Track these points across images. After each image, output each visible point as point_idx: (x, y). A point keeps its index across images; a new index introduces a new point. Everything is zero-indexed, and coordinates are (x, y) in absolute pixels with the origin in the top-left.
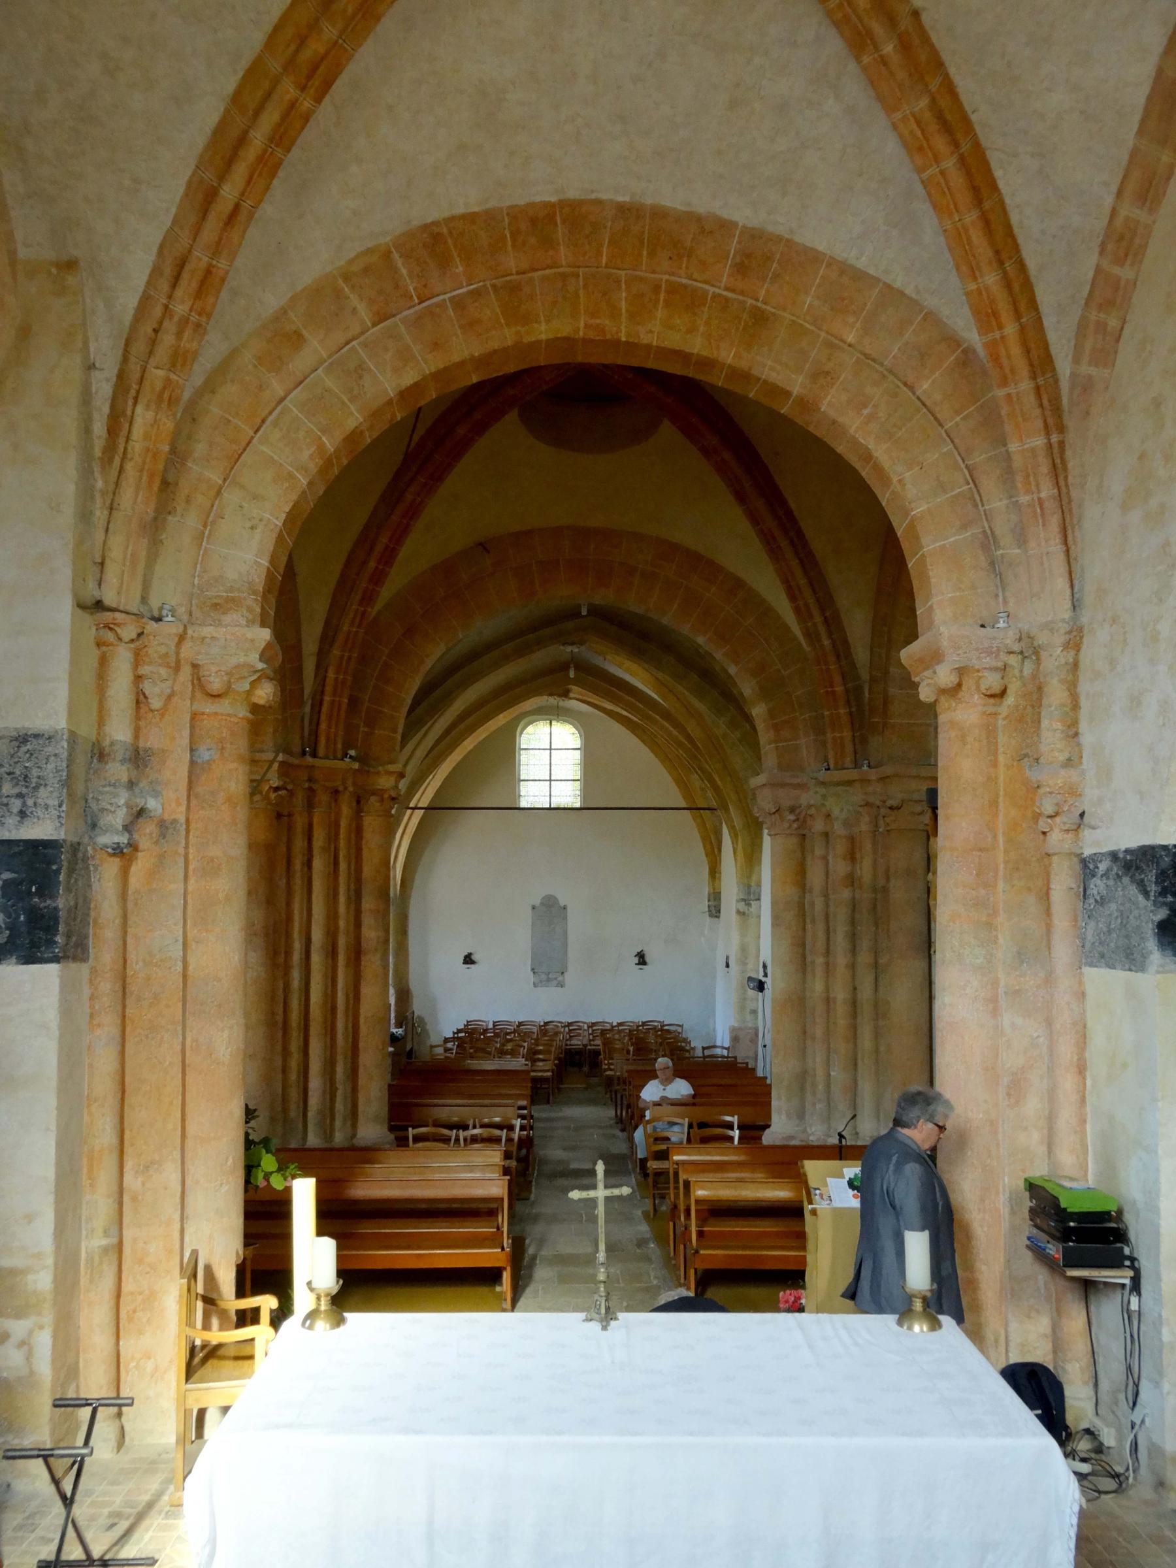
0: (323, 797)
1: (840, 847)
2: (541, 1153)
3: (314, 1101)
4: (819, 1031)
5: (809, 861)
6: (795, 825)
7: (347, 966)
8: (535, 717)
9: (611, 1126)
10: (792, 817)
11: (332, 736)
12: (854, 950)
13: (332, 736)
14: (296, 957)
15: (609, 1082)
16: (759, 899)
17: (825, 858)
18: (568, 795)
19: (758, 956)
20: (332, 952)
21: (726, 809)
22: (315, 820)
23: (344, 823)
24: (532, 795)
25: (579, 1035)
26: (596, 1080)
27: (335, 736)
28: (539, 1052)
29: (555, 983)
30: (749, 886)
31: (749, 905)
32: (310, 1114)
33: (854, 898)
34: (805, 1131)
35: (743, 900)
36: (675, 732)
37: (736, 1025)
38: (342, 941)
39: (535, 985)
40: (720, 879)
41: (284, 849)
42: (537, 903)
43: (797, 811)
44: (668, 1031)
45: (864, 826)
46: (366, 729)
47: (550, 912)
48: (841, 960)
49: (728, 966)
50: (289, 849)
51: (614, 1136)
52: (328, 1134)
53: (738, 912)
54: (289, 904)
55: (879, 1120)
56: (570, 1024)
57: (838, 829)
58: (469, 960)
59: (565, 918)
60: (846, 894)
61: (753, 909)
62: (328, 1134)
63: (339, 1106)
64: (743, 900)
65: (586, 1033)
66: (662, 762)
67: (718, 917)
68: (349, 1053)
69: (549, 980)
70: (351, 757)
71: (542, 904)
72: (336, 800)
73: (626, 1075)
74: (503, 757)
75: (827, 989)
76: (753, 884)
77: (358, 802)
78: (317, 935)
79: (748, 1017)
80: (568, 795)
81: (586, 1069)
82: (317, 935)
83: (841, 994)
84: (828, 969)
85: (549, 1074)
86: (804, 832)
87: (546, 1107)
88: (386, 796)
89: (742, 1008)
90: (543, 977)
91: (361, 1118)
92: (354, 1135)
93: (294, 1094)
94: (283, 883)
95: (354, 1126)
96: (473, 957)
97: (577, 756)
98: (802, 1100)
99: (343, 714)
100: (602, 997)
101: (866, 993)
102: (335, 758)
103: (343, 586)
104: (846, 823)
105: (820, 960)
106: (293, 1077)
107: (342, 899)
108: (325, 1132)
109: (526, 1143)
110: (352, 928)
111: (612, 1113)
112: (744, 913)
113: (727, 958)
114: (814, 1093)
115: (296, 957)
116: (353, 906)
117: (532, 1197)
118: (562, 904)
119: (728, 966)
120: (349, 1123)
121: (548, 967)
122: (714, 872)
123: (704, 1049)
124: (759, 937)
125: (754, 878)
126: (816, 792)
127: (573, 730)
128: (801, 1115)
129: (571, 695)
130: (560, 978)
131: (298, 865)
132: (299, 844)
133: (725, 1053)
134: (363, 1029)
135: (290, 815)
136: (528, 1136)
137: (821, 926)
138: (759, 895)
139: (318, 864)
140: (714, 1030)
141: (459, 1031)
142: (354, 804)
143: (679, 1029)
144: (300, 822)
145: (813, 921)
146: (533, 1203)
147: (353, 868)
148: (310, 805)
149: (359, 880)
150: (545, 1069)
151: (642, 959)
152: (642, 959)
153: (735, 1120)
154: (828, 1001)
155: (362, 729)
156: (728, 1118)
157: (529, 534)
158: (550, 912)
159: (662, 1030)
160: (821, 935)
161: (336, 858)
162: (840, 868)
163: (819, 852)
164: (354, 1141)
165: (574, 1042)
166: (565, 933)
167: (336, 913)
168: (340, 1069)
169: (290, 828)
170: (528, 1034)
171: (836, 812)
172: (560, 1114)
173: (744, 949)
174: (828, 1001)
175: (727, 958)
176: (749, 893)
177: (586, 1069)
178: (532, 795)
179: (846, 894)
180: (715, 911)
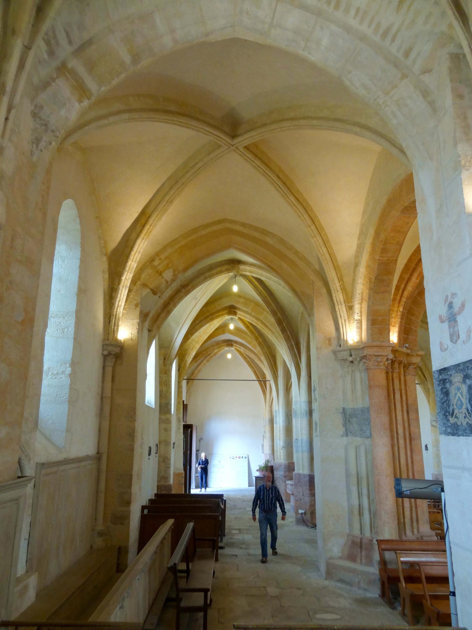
35: (435, 421)
46: (405, 336)
53: (432, 426)
64: (435, 421)
70: (406, 347)
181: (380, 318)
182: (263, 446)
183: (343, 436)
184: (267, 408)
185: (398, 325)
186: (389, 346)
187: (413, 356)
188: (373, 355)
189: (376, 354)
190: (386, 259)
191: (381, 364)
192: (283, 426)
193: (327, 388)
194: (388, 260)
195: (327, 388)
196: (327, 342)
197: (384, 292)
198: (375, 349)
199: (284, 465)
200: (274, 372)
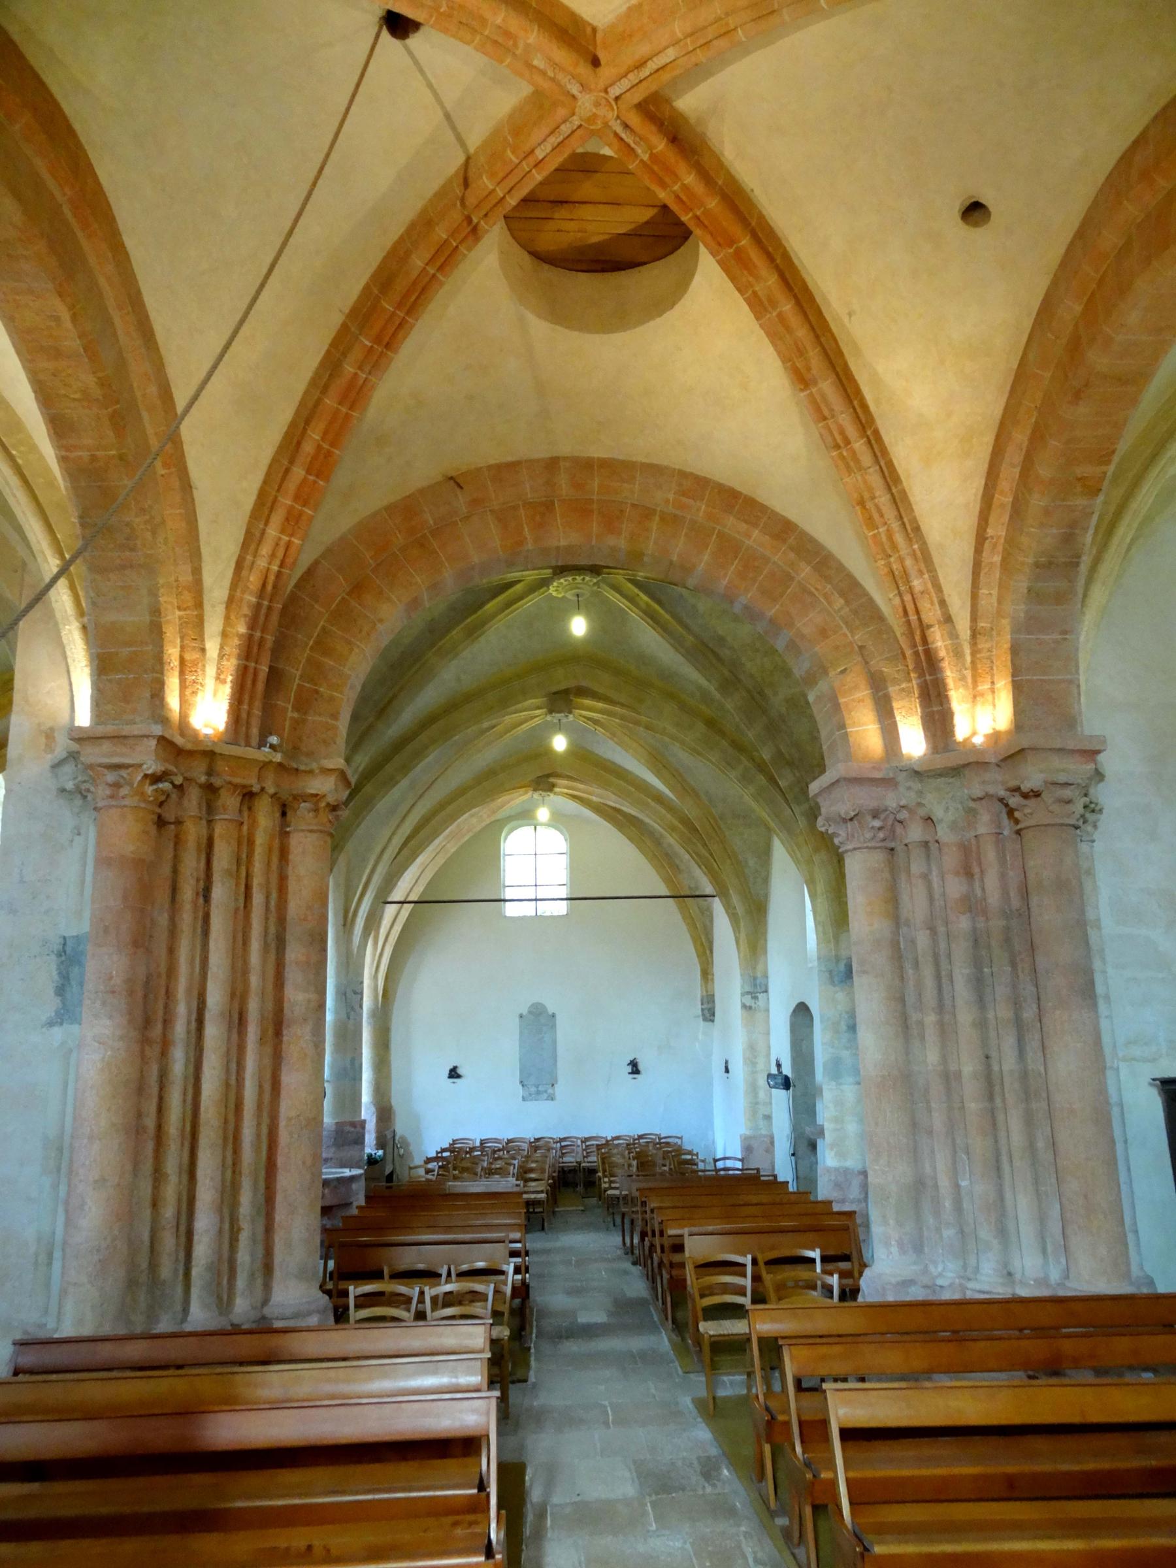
0: (229, 802)
1: (951, 859)
2: (539, 1299)
3: (202, 1250)
4: (938, 1121)
5: (903, 884)
6: (881, 835)
7: (262, 1040)
8: (520, 822)
9: (619, 1258)
10: (877, 823)
11: (244, 715)
12: (981, 1002)
13: (244, 715)
14: (180, 1028)
15: (612, 1204)
16: (766, 991)
17: (926, 877)
19: (768, 1055)
20: (238, 1021)
22: (219, 830)
23: (260, 839)
25: (572, 1151)
26: (594, 1201)
27: (249, 714)
28: (532, 1170)
29: (545, 1096)
30: (755, 979)
31: (755, 998)
32: (195, 1272)
33: (974, 930)
34: (925, 1271)
35: (748, 993)
36: (669, 816)
37: (748, 1133)
38: (253, 1007)
39: (524, 1099)
40: (713, 980)
41: (166, 870)
42: (525, 1012)
43: (882, 816)
44: (668, 1144)
45: (984, 825)
46: (296, 715)
47: (538, 1022)
48: (965, 1016)
49: (727, 1071)
50: (175, 871)
51: (626, 1272)
52: (223, 1303)
53: (744, 1006)
54: (171, 951)
55: (1044, 1251)
56: (564, 1139)
57: (944, 833)
58: (454, 1074)
59: (554, 1026)
60: (964, 923)
61: (761, 1002)
62: (223, 1303)
63: (244, 1257)
64: (748, 993)
65: (580, 1149)
66: (651, 861)
67: (713, 1021)
68: (262, 1174)
69: (538, 1093)
70: (272, 747)
71: (530, 1012)
72: (250, 809)
73: (637, 1194)
74: (484, 854)
75: (944, 1059)
76: (759, 975)
77: (284, 814)
78: (215, 998)
79: (762, 1123)
81: (580, 1189)
82: (215, 998)
83: (968, 1067)
84: (946, 1031)
85: (543, 1195)
86: (892, 845)
87: (543, 1234)
88: (323, 804)
89: (754, 1112)
90: (533, 1089)
91: (277, 1273)
92: (266, 1302)
93: (168, 1241)
94: (163, 920)
95: (267, 1287)
96: (459, 1071)
97: (564, 861)
98: (918, 1219)
99: (260, 686)
100: (598, 1110)
101: (1008, 1063)
102: (248, 745)
103: (264, 505)
104: (954, 826)
105: (931, 1019)
106: (169, 1212)
107: (255, 945)
108: (219, 1298)
109: (522, 1291)
110: (270, 987)
111: (618, 1239)
112: (750, 1008)
113: (726, 1062)
114: (937, 1213)
115: (180, 1028)
116: (272, 957)
117: (532, 1378)
119: (727, 1071)
120: (259, 1281)
121: (538, 1079)
124: (768, 1034)
125: (760, 967)
126: (909, 788)
128: (918, 1246)
129: (557, 790)
130: (550, 1091)
131: (188, 892)
132: (191, 864)
133: (739, 1165)
134: (284, 1137)
135: (179, 822)
136: (523, 1281)
137: (928, 972)
139: (220, 892)
140: (713, 1142)
141: (443, 1150)
142: (278, 815)
143: (679, 1141)
144: (193, 832)
145: (916, 965)
146: (534, 1385)
147: (273, 903)
148: (210, 808)
149: (282, 921)
150: (538, 1190)
151: (635, 1068)
152: (635, 1068)
153: (815, 1254)
154: (950, 1078)
155: (290, 714)
156: (810, 1254)
157: (513, 466)
158: (538, 1022)
159: (660, 1143)
160: (929, 982)
161: (248, 888)
162: (955, 887)
163: (917, 867)
164: (267, 1311)
165: (565, 1159)
166: (554, 1042)
167: (246, 962)
168: (246, 1198)
169: (178, 842)
170: (519, 1149)
171: (938, 813)
172: (558, 1244)
173: (751, 1048)
174: (950, 1078)
175: (726, 1062)
176: (755, 985)
177: (580, 1189)
179: (964, 923)
180: (709, 1014)
181: (125, 651)
183: (51, 1024)
185: (230, 678)
186: (147, 737)
187: (311, 772)
188: (100, 765)
189: (116, 760)
190: (85, 454)
191: (124, 791)
193: (22, 881)
194: (94, 459)
195: (22, 881)
196: (43, 740)
197: (123, 567)
198: (106, 746)
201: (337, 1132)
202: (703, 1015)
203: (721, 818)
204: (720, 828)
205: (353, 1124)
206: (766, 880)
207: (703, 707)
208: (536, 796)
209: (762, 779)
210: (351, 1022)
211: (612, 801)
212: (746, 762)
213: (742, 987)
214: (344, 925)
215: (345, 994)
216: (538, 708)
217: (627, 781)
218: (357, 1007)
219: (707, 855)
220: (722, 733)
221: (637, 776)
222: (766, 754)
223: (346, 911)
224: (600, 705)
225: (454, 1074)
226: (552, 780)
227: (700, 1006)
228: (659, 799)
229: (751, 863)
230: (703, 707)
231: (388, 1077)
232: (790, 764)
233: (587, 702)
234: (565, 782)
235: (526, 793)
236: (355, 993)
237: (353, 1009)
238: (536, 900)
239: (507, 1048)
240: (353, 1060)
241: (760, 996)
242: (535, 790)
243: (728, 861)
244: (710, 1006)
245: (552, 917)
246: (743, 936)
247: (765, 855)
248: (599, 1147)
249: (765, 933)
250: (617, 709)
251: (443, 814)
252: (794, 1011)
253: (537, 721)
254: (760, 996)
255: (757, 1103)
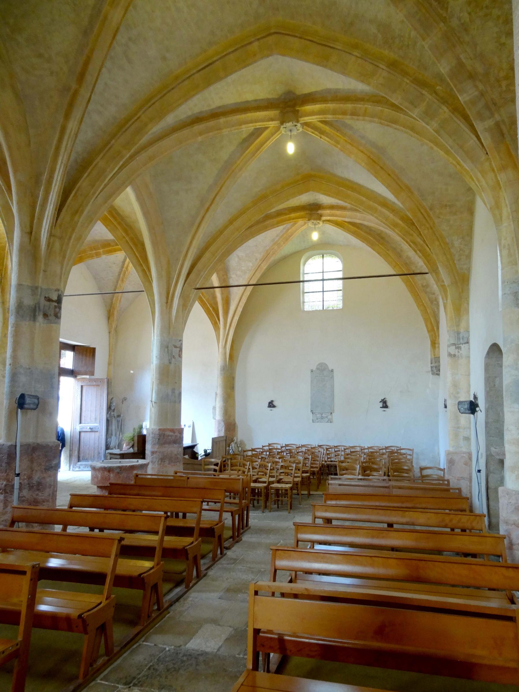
16: (468, 343)
18: (334, 300)
21: (435, 271)
24: (312, 302)
29: (326, 420)
30: (458, 333)
31: (459, 348)
35: (454, 344)
36: (391, 216)
37: (451, 449)
39: (313, 421)
40: (439, 347)
42: (314, 369)
47: (323, 374)
49: (446, 407)
53: (450, 355)
58: (271, 405)
59: (332, 377)
64: (454, 344)
67: (439, 375)
69: (322, 418)
71: (317, 369)
76: (462, 330)
79: (462, 443)
80: (334, 300)
89: (456, 436)
96: (275, 403)
112: (455, 355)
118: (330, 369)
119: (446, 407)
121: (322, 409)
122: (434, 344)
123: (422, 469)
124: (469, 375)
125: (463, 324)
127: (337, 259)
129: (324, 218)
130: (330, 417)
138: (468, 339)
143: (409, 452)
151: (385, 404)
152: (385, 404)
158: (323, 374)
166: (333, 387)
176: (459, 339)
178: (312, 302)
182: (214, 408)
184: (220, 350)
192: (156, 365)
199: (152, 433)
200: (144, 271)
201: (160, 435)
202: (432, 371)
203: (431, 209)
204: (429, 216)
205: (172, 431)
206: (469, 257)
207: (386, 52)
208: (310, 224)
209: (445, 111)
210: (172, 366)
211: (359, 218)
212: (428, 96)
213: (449, 340)
214: (167, 303)
215: (167, 347)
216: (272, 120)
217: (359, 193)
218: (177, 356)
219: (422, 242)
220: (405, 74)
221: (368, 189)
222: (444, 68)
223: (168, 293)
224: (316, 107)
225: (271, 405)
226: (320, 212)
227: (430, 365)
228: (385, 203)
229: (456, 244)
230: (386, 52)
231: (233, 406)
232: (472, 76)
233: (308, 108)
234: (328, 212)
235: (305, 223)
236: (176, 347)
237: (174, 357)
238: (323, 301)
239: (304, 390)
240: (173, 390)
241: (462, 346)
242: (309, 220)
243: (437, 243)
244: (436, 364)
245: (333, 310)
246: (449, 301)
247: (468, 235)
248: (392, 452)
249: (467, 298)
250: (331, 106)
251: (232, 227)
252: (488, 353)
253: (276, 137)
254: (462, 346)
255: (458, 428)
